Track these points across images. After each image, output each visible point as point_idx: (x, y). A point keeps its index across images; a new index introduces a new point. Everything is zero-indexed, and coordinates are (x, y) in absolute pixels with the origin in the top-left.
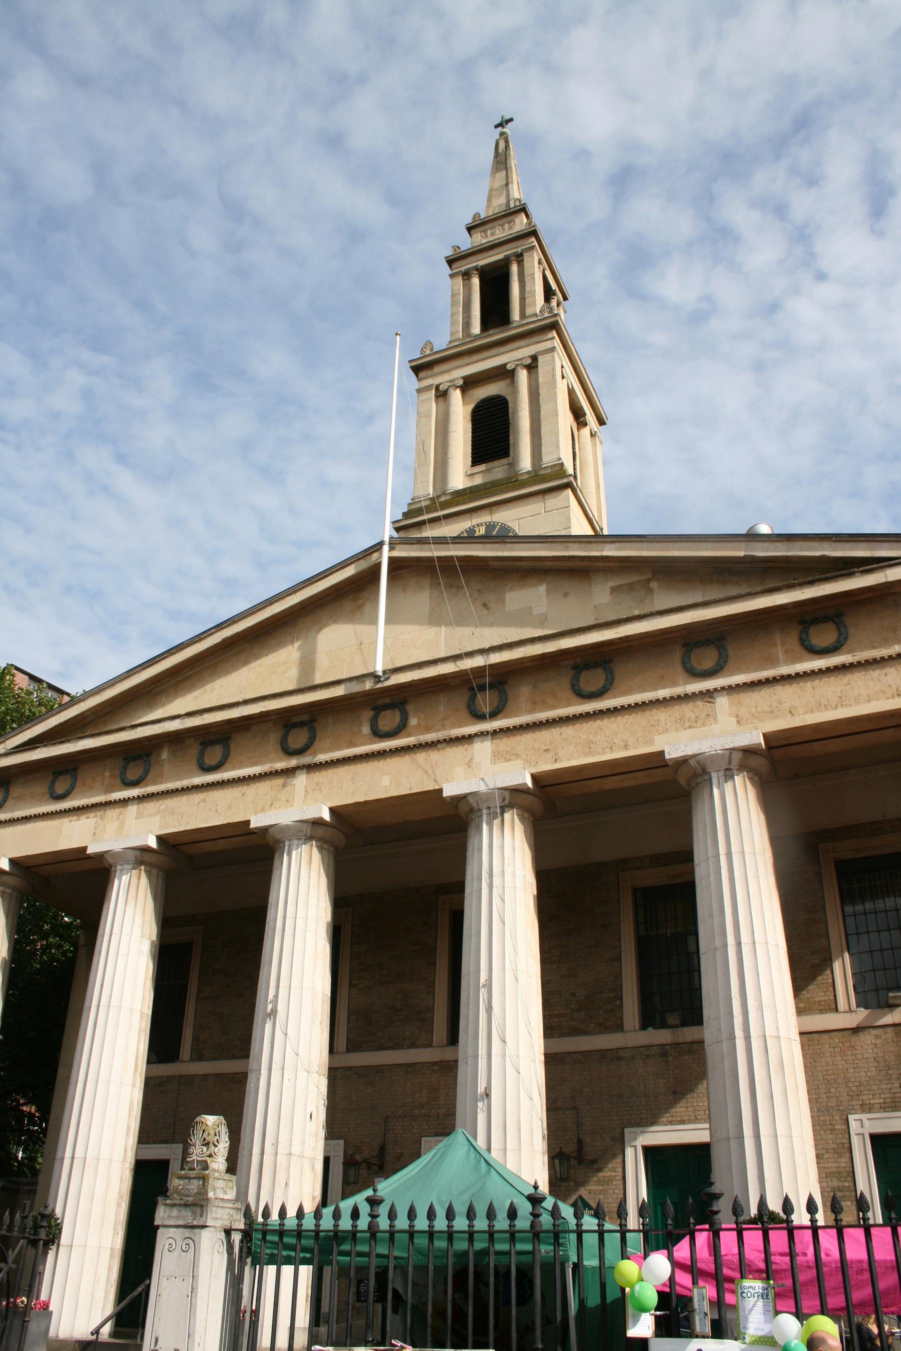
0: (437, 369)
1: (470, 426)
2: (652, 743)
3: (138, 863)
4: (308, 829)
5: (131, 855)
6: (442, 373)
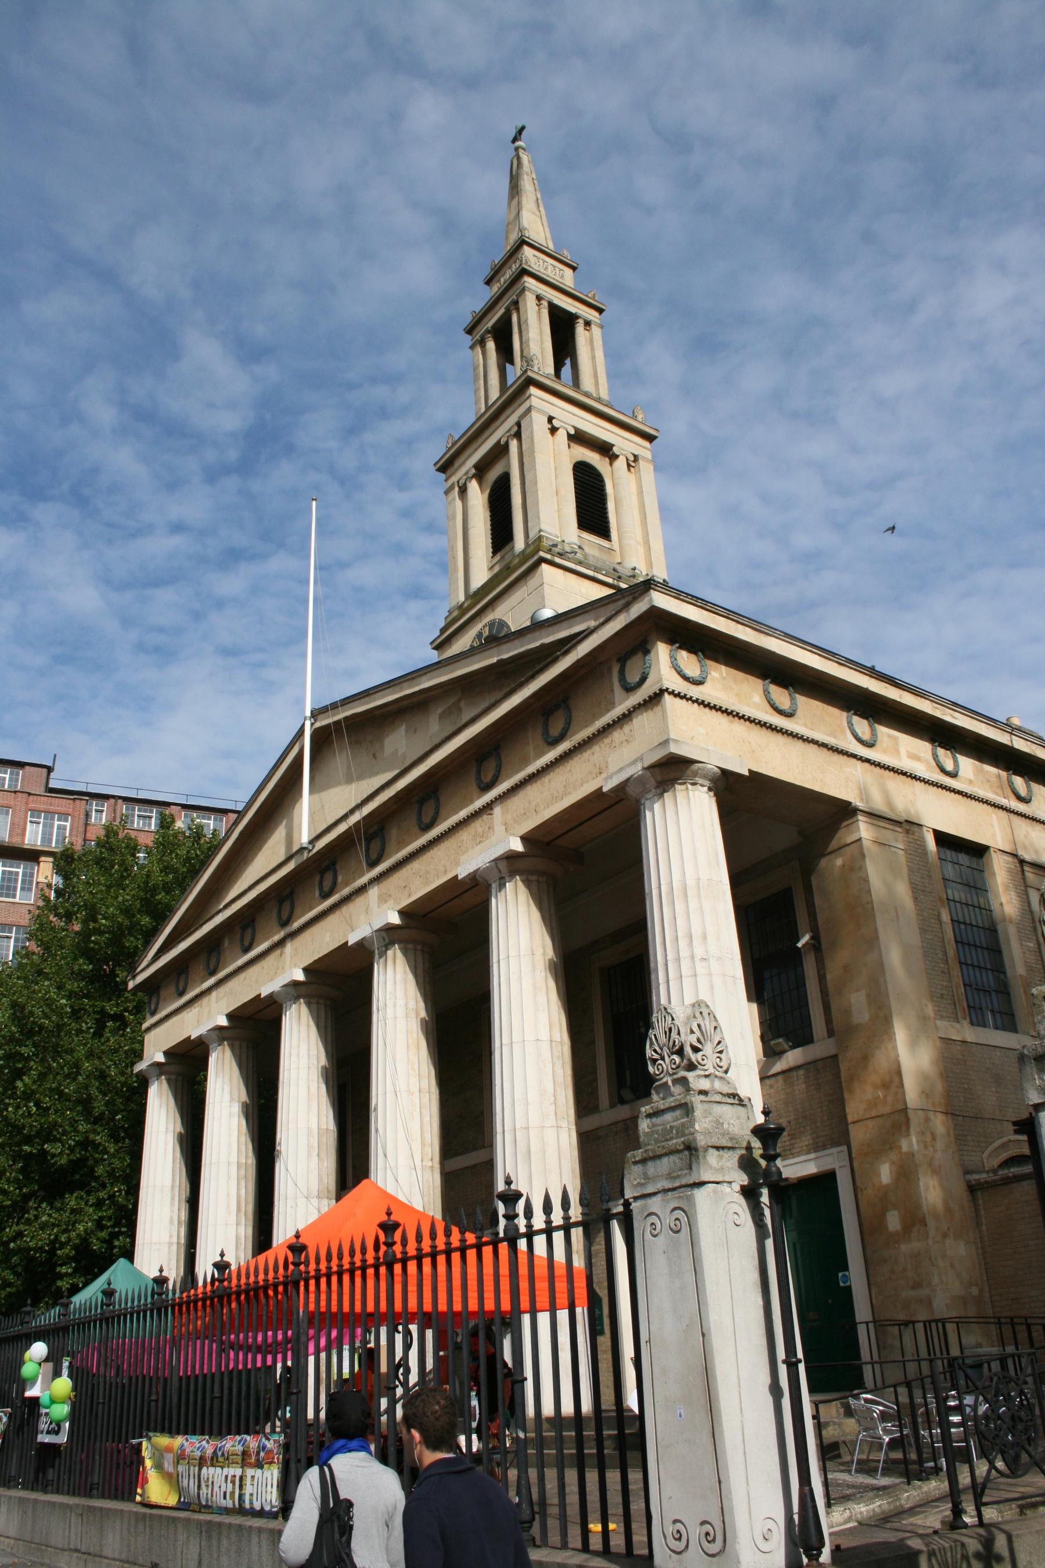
0: (457, 464)
1: (488, 514)
2: (457, 864)
3: (221, 1040)
4: (292, 991)
5: (214, 1035)
6: (460, 466)
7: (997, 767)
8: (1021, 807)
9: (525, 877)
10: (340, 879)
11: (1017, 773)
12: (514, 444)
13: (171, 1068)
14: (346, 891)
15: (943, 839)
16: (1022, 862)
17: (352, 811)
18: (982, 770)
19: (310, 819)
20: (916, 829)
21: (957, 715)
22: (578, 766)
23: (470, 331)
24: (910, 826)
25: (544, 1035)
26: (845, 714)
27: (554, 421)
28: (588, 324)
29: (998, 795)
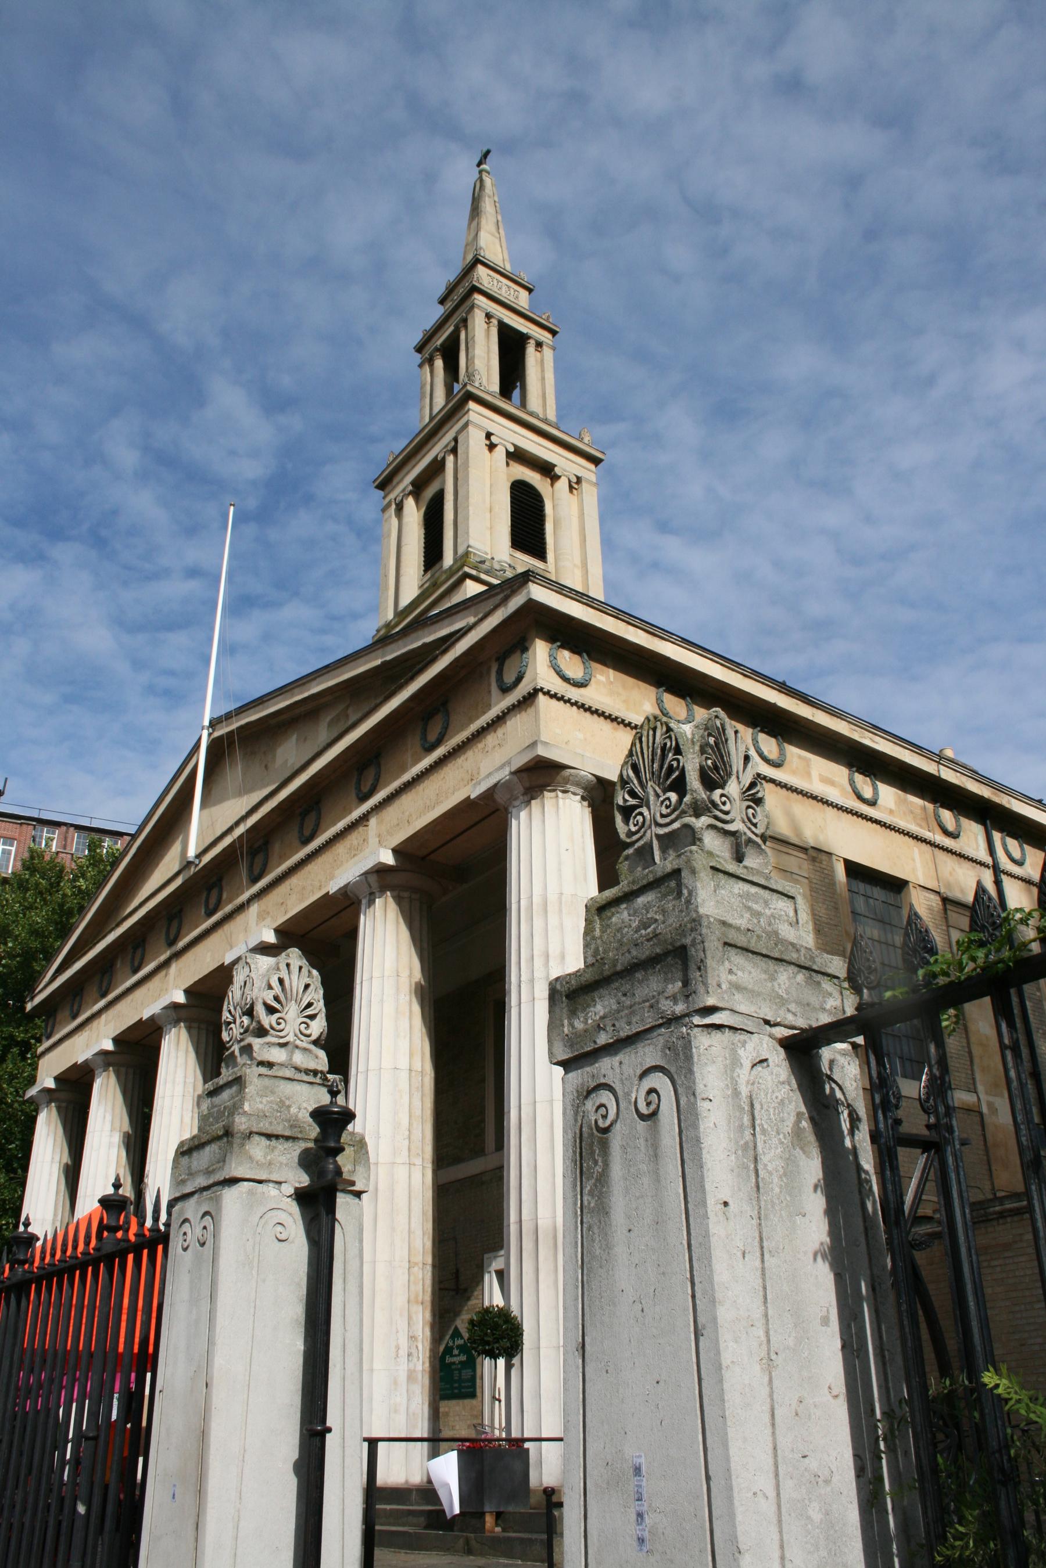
0: (395, 482)
1: (423, 531)
2: (332, 877)
3: (106, 1066)
4: (173, 1014)
5: (100, 1060)
6: (398, 483)
7: (922, 798)
8: (948, 842)
9: (396, 893)
10: (225, 896)
11: (942, 806)
12: (450, 459)
13: (63, 1095)
14: (228, 908)
15: (854, 870)
16: (945, 900)
17: (237, 824)
18: (905, 800)
19: (201, 833)
20: (824, 857)
21: (877, 739)
22: (451, 773)
23: (419, 349)
24: (817, 855)
25: (404, 1063)
26: (750, 730)
27: (493, 438)
28: (539, 345)
29: (921, 826)
